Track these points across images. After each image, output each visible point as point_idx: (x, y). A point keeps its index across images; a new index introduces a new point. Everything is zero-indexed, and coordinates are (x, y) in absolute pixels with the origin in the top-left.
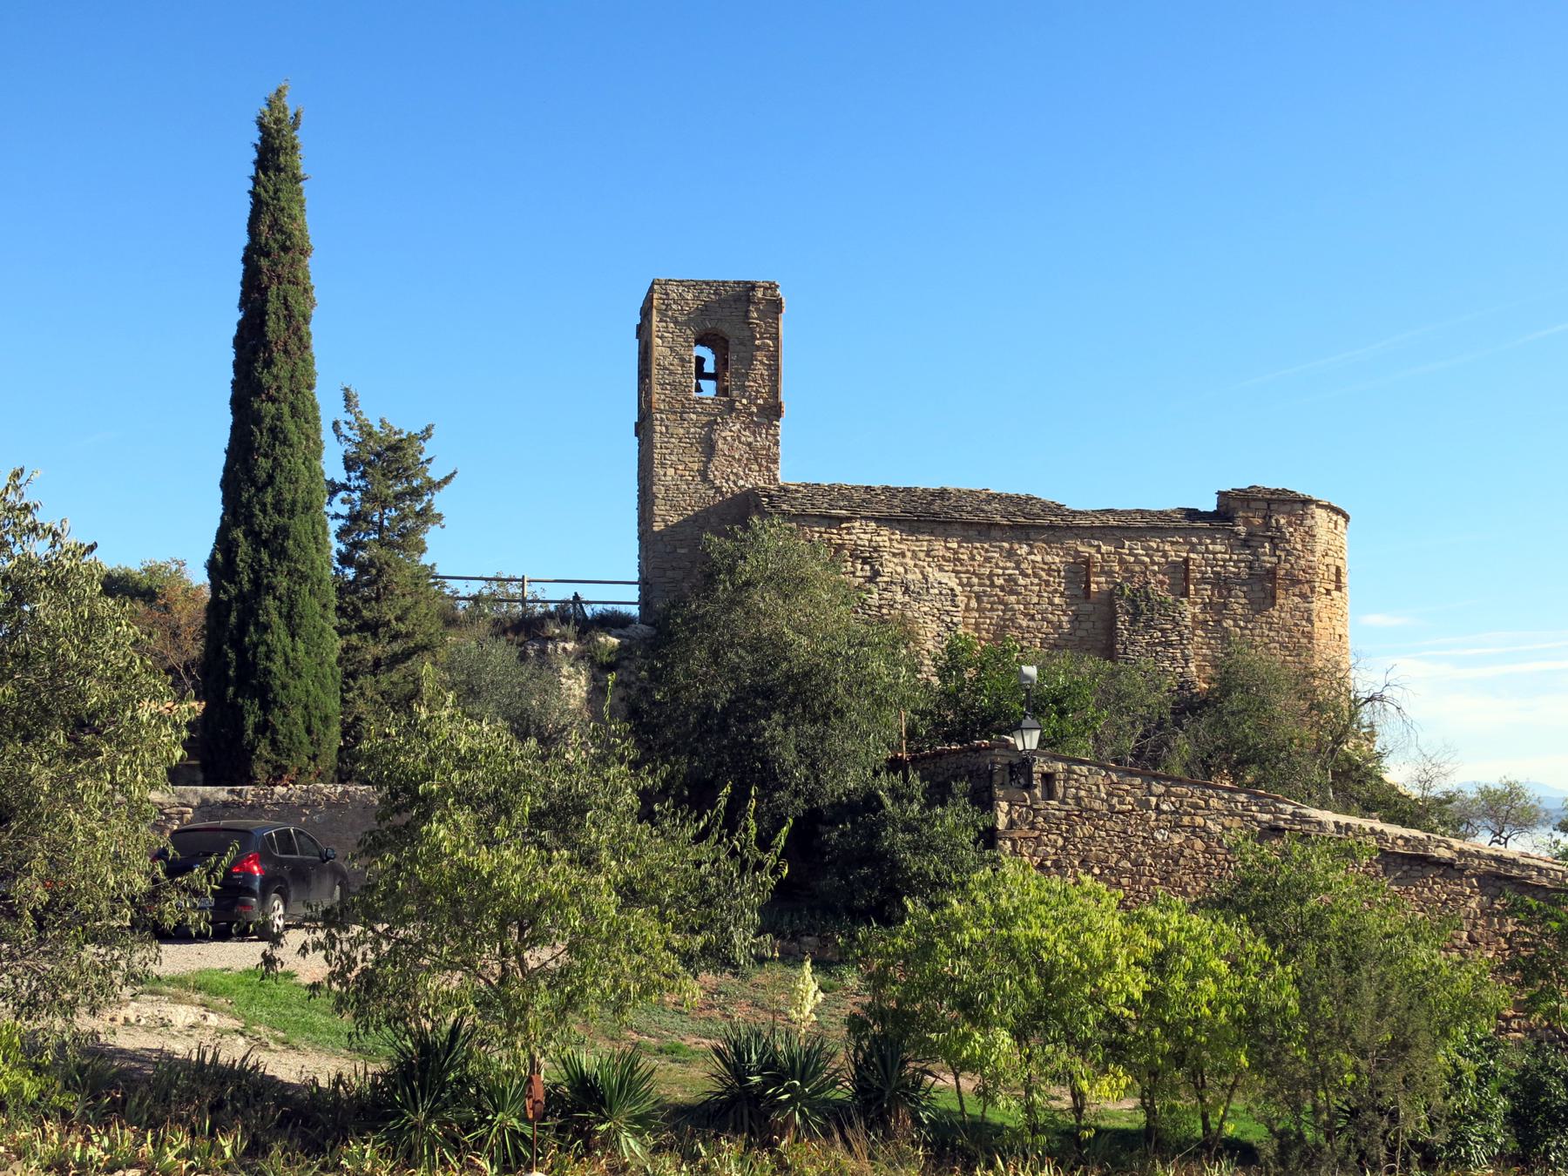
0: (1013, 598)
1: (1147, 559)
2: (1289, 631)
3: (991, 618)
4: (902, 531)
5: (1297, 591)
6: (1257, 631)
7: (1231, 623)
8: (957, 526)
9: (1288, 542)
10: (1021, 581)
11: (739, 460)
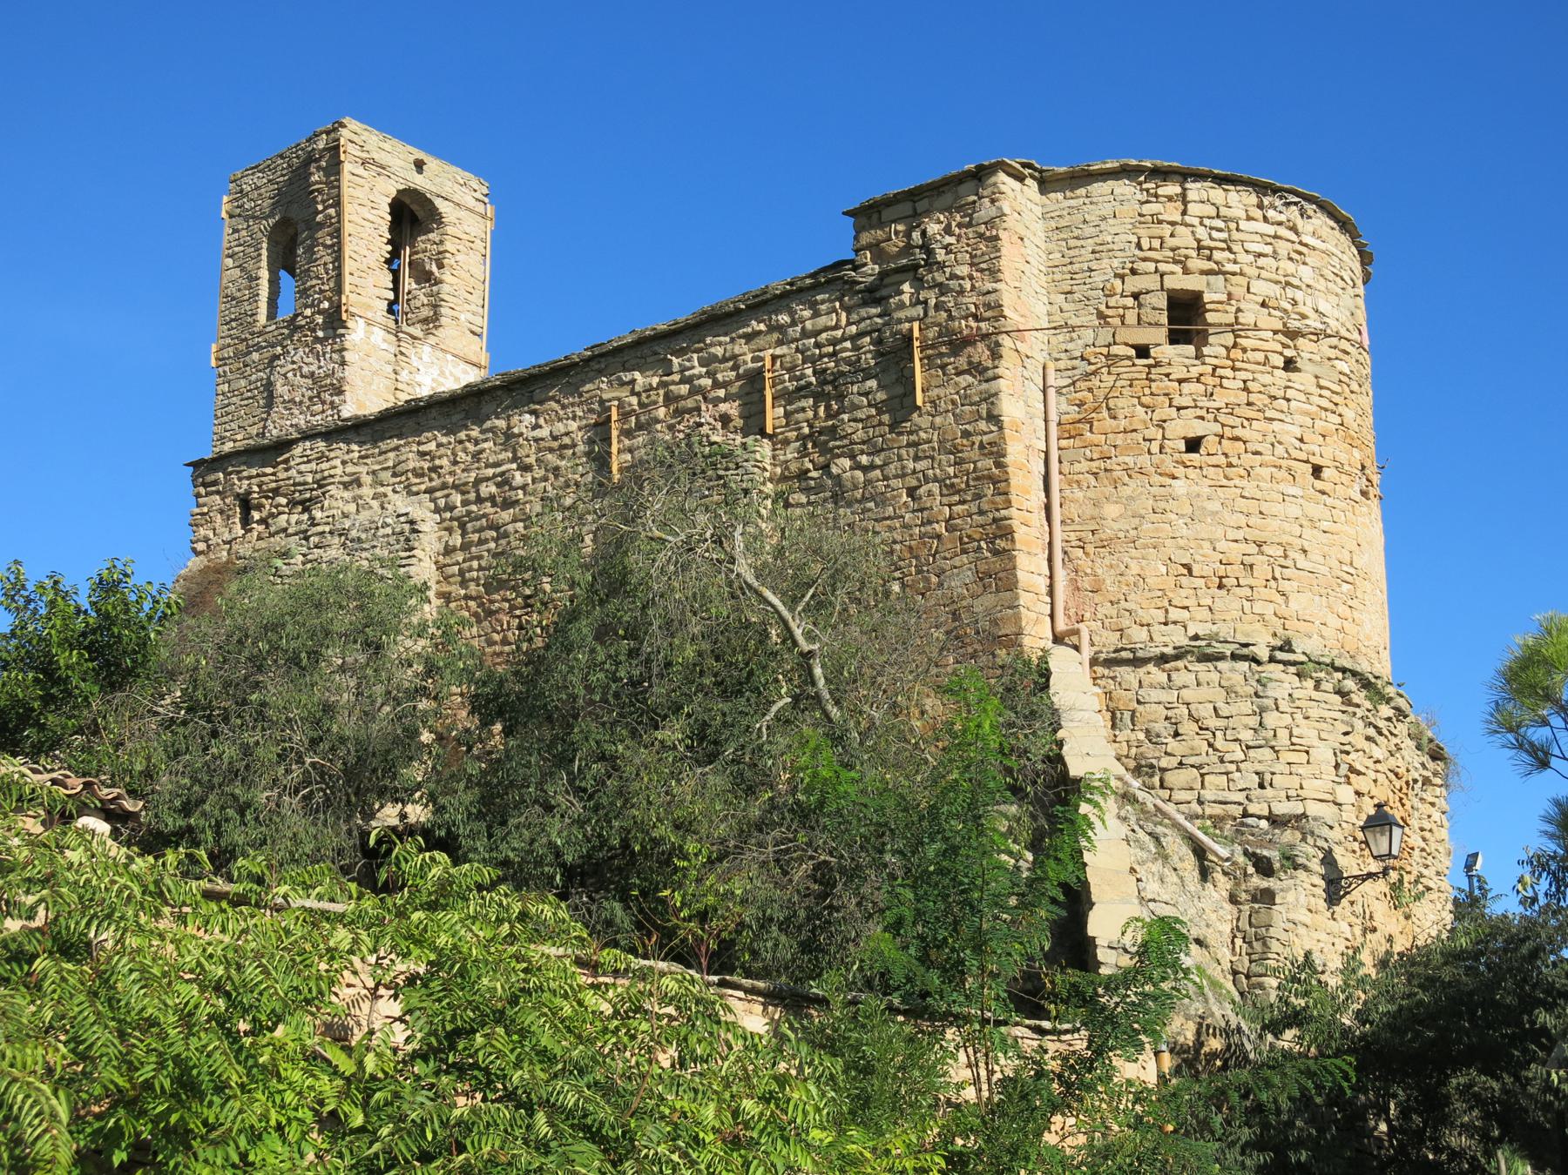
0: (506, 516)
1: (707, 382)
2: (955, 450)
3: (479, 558)
4: (361, 444)
5: (962, 362)
6: (892, 469)
7: (847, 463)
8: (434, 412)
9: (941, 266)
10: (518, 479)
11: (301, 402)
